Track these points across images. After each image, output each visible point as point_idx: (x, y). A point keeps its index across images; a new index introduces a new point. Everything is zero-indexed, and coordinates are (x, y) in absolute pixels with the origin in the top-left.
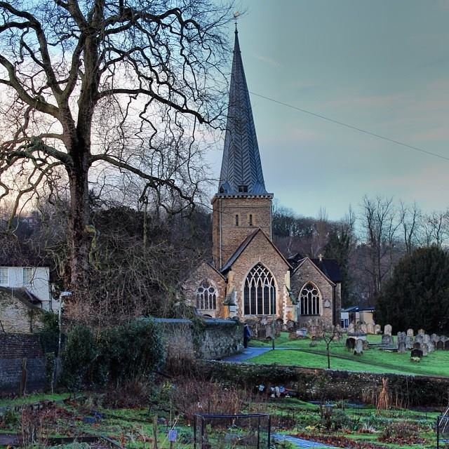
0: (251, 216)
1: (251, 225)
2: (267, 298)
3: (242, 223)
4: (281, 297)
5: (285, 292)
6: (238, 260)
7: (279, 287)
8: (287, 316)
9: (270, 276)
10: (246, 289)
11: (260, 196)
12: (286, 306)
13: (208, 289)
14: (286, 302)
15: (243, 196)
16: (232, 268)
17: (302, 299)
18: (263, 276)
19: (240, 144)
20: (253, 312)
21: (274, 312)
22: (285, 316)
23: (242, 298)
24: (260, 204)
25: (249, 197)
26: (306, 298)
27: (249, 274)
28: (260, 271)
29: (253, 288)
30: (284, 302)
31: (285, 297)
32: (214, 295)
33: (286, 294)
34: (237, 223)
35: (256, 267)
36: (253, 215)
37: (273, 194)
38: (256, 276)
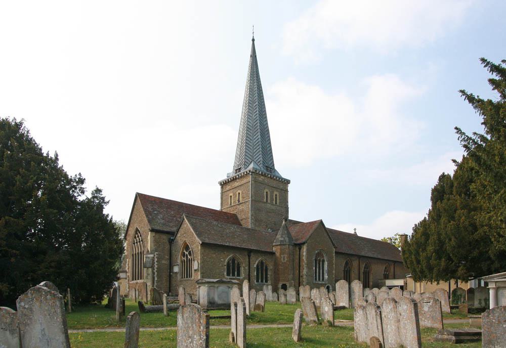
0: (239, 194)
1: (239, 202)
34: (231, 202)
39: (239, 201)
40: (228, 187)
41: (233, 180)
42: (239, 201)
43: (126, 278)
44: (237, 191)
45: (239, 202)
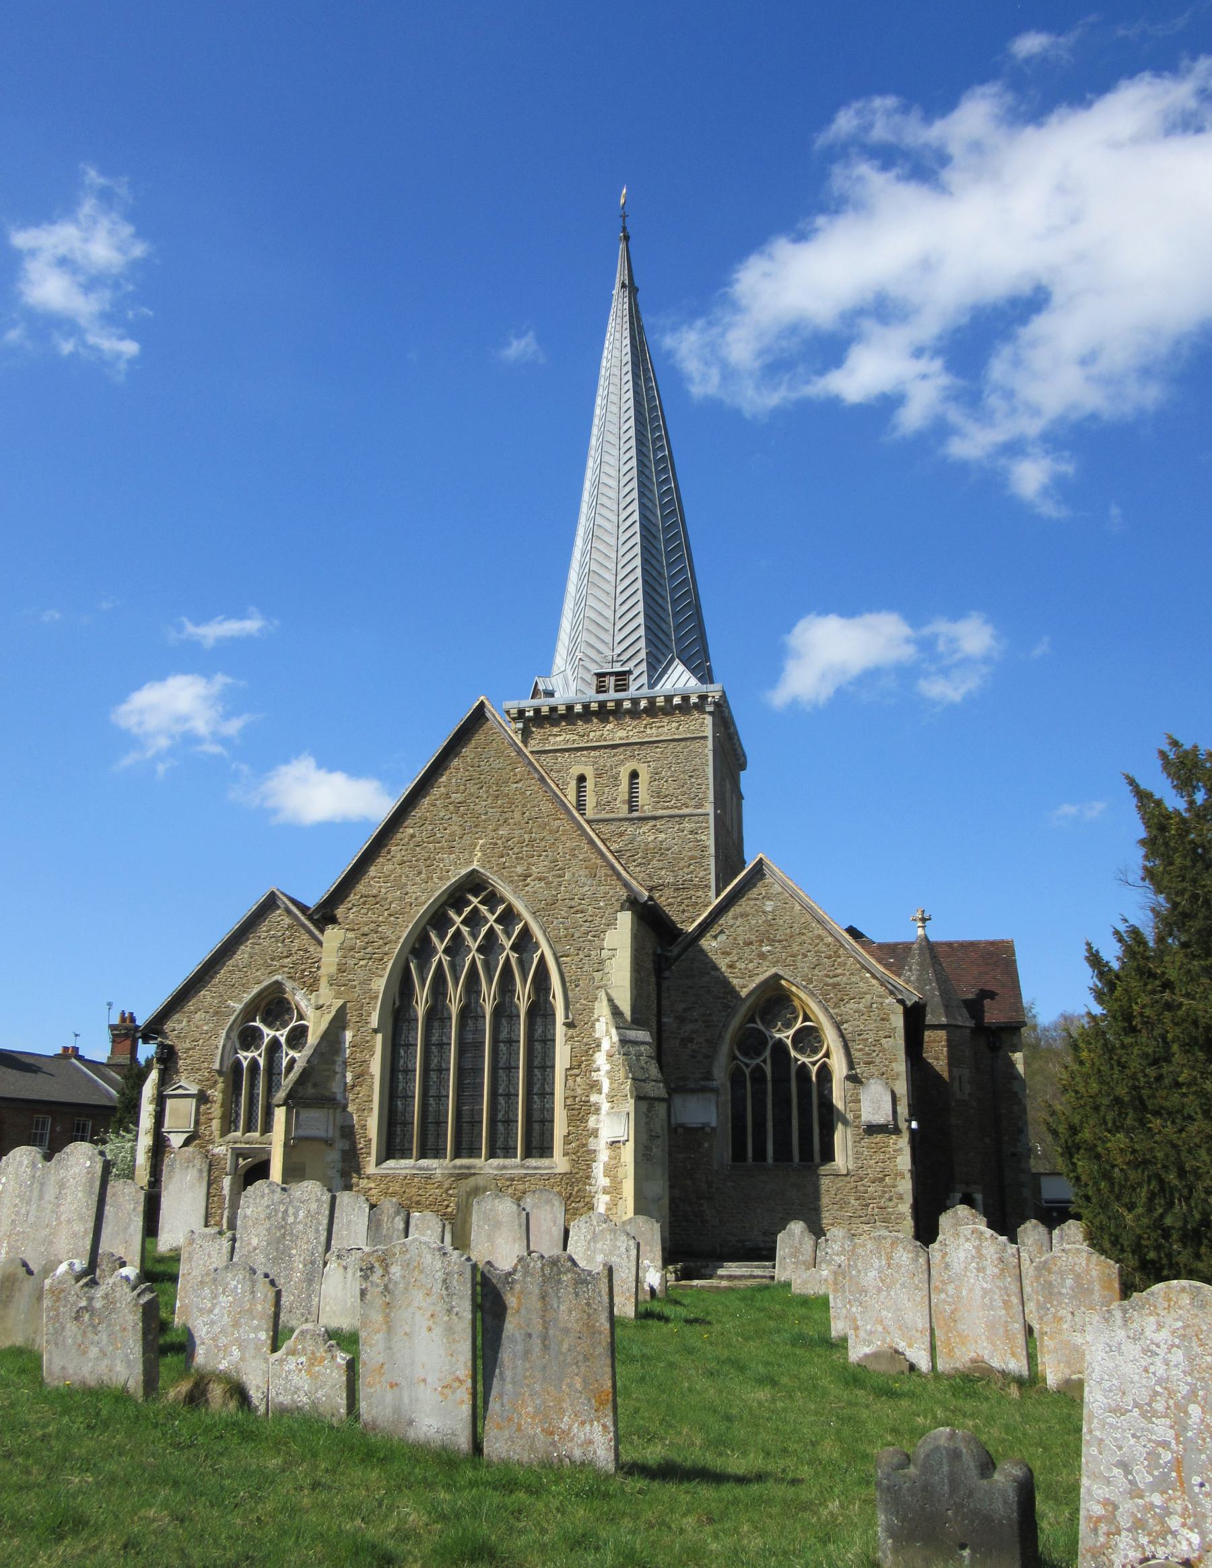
0: (634, 775)
2: (505, 1068)
4: (582, 1063)
9: (525, 942)
12: (605, 1107)
13: (282, 1035)
15: (602, 704)
17: (736, 1078)
18: (489, 946)
20: (431, 1149)
21: (539, 1145)
22: (598, 1169)
26: (759, 1069)
29: (436, 1014)
30: (595, 1086)
31: (601, 1059)
33: (606, 1034)
35: (456, 898)
38: (456, 948)
39: (632, 804)
40: (560, 737)
41: (596, 714)
42: (632, 804)
43: (328, 1143)
44: (622, 762)
45: (631, 811)
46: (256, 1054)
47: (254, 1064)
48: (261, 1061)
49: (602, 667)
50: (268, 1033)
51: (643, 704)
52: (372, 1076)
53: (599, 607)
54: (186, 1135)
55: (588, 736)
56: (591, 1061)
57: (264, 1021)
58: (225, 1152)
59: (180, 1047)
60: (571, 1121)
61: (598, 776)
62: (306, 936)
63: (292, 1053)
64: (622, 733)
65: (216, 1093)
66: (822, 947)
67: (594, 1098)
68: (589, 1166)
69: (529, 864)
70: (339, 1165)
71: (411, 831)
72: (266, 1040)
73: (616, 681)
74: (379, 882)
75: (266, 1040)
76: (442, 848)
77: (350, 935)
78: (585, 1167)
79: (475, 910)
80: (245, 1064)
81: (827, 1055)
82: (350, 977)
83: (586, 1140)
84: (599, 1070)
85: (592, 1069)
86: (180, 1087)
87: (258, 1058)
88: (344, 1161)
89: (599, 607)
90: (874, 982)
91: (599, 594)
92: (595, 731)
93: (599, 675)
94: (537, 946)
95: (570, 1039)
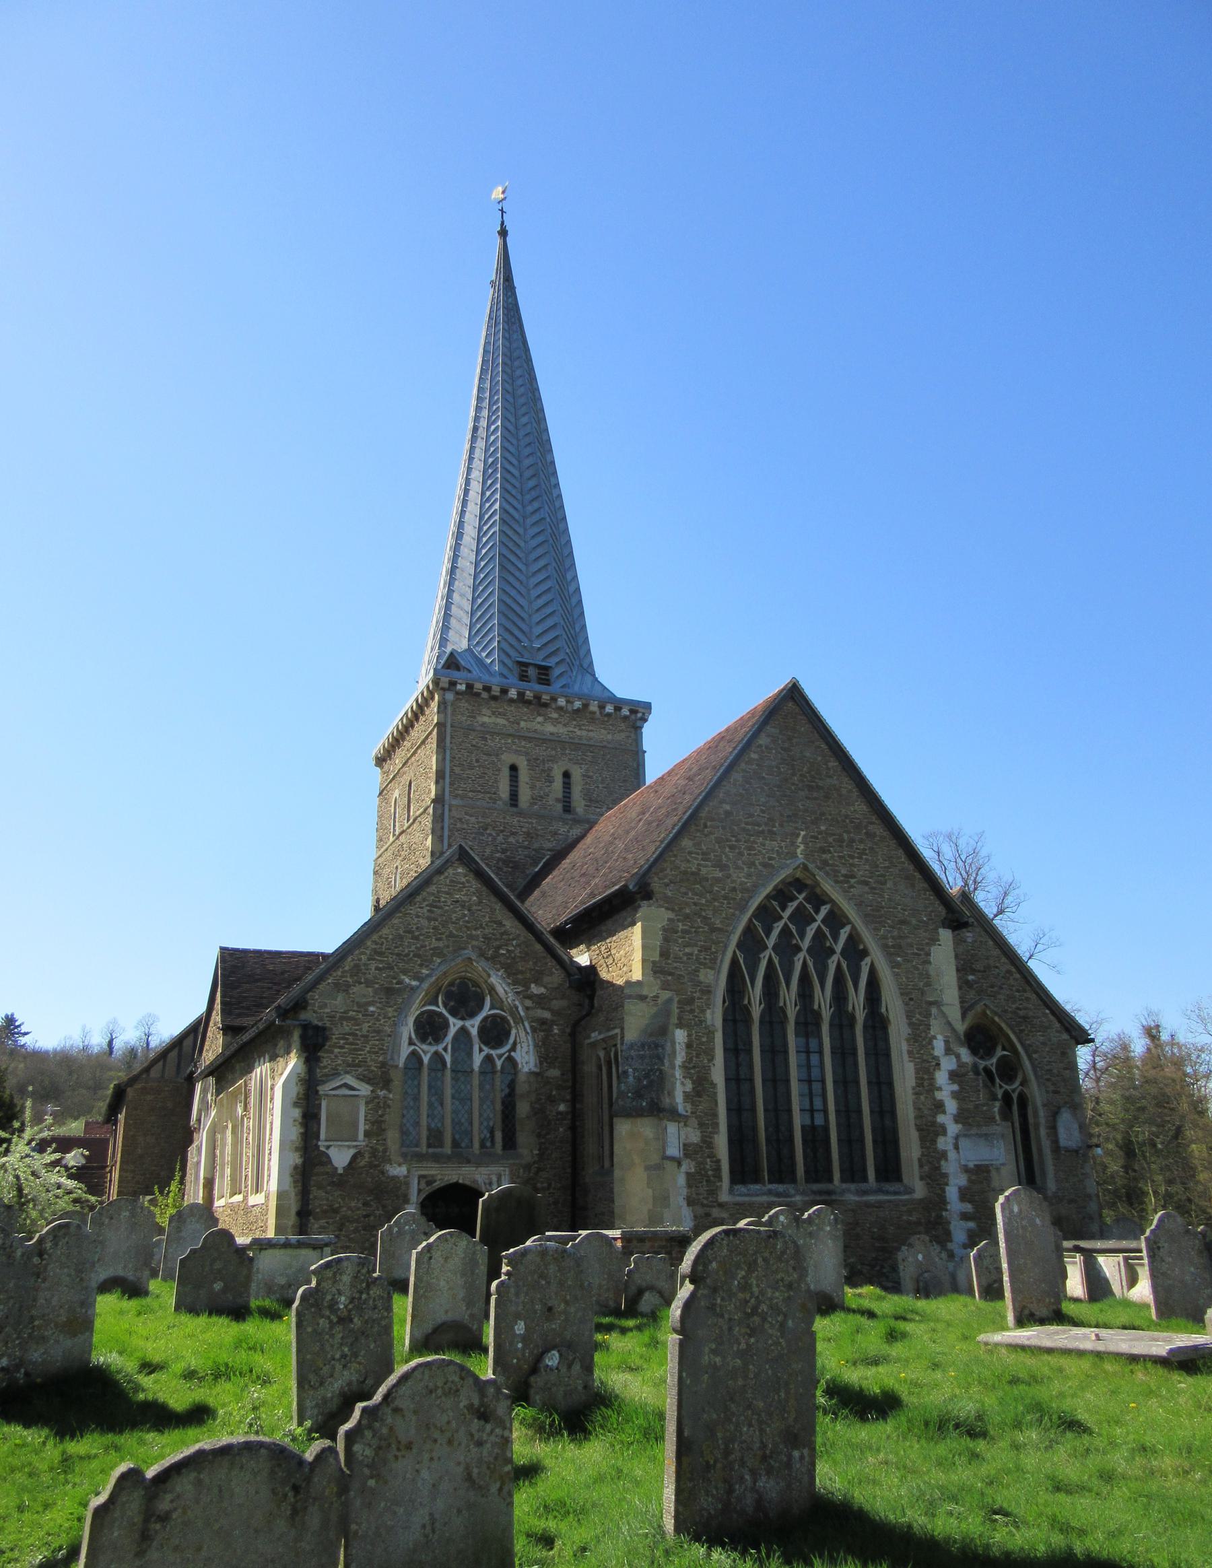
0: (566, 775)
3: (534, 800)
4: (925, 1083)
5: (939, 1046)
6: (686, 843)
7: (909, 1015)
8: (964, 1195)
9: (855, 951)
10: (736, 1014)
11: (602, 707)
12: (953, 1129)
14: (951, 1106)
16: (656, 885)
19: (521, 531)
21: (890, 1170)
22: (952, 1193)
23: (718, 1075)
24: (600, 735)
25: (562, 702)
27: (749, 930)
28: (800, 918)
30: (939, 1107)
31: (941, 1078)
32: (511, 1060)
36: (577, 773)
37: (648, 706)
38: (787, 947)
41: (529, 703)
44: (553, 759)
46: (440, 1048)
47: (438, 1058)
48: (448, 1058)
49: (522, 656)
50: (455, 1025)
51: (578, 704)
52: (714, 1085)
53: (513, 593)
54: (352, 1152)
55: (518, 724)
56: (932, 1079)
57: (445, 1005)
58: (406, 1173)
59: (336, 1033)
60: (923, 1139)
61: (531, 767)
62: (498, 906)
63: (486, 1050)
64: (550, 728)
65: (391, 1096)
66: (1012, 982)
67: (941, 1119)
68: (944, 1191)
69: (852, 865)
70: (685, 1192)
71: (728, 807)
72: (452, 1031)
73: (539, 674)
74: (696, 859)
75: (452, 1031)
76: (763, 832)
77: (671, 915)
78: (940, 1192)
79: (799, 909)
80: (426, 1059)
81: (1024, 1083)
82: (675, 965)
83: (939, 1162)
84: (940, 1089)
85: (932, 1088)
86: (346, 1086)
87: (443, 1053)
88: (689, 1186)
89: (513, 593)
90: (1052, 1017)
91: (511, 579)
92: (525, 721)
93: (520, 664)
94: (865, 953)
95: (910, 1053)
